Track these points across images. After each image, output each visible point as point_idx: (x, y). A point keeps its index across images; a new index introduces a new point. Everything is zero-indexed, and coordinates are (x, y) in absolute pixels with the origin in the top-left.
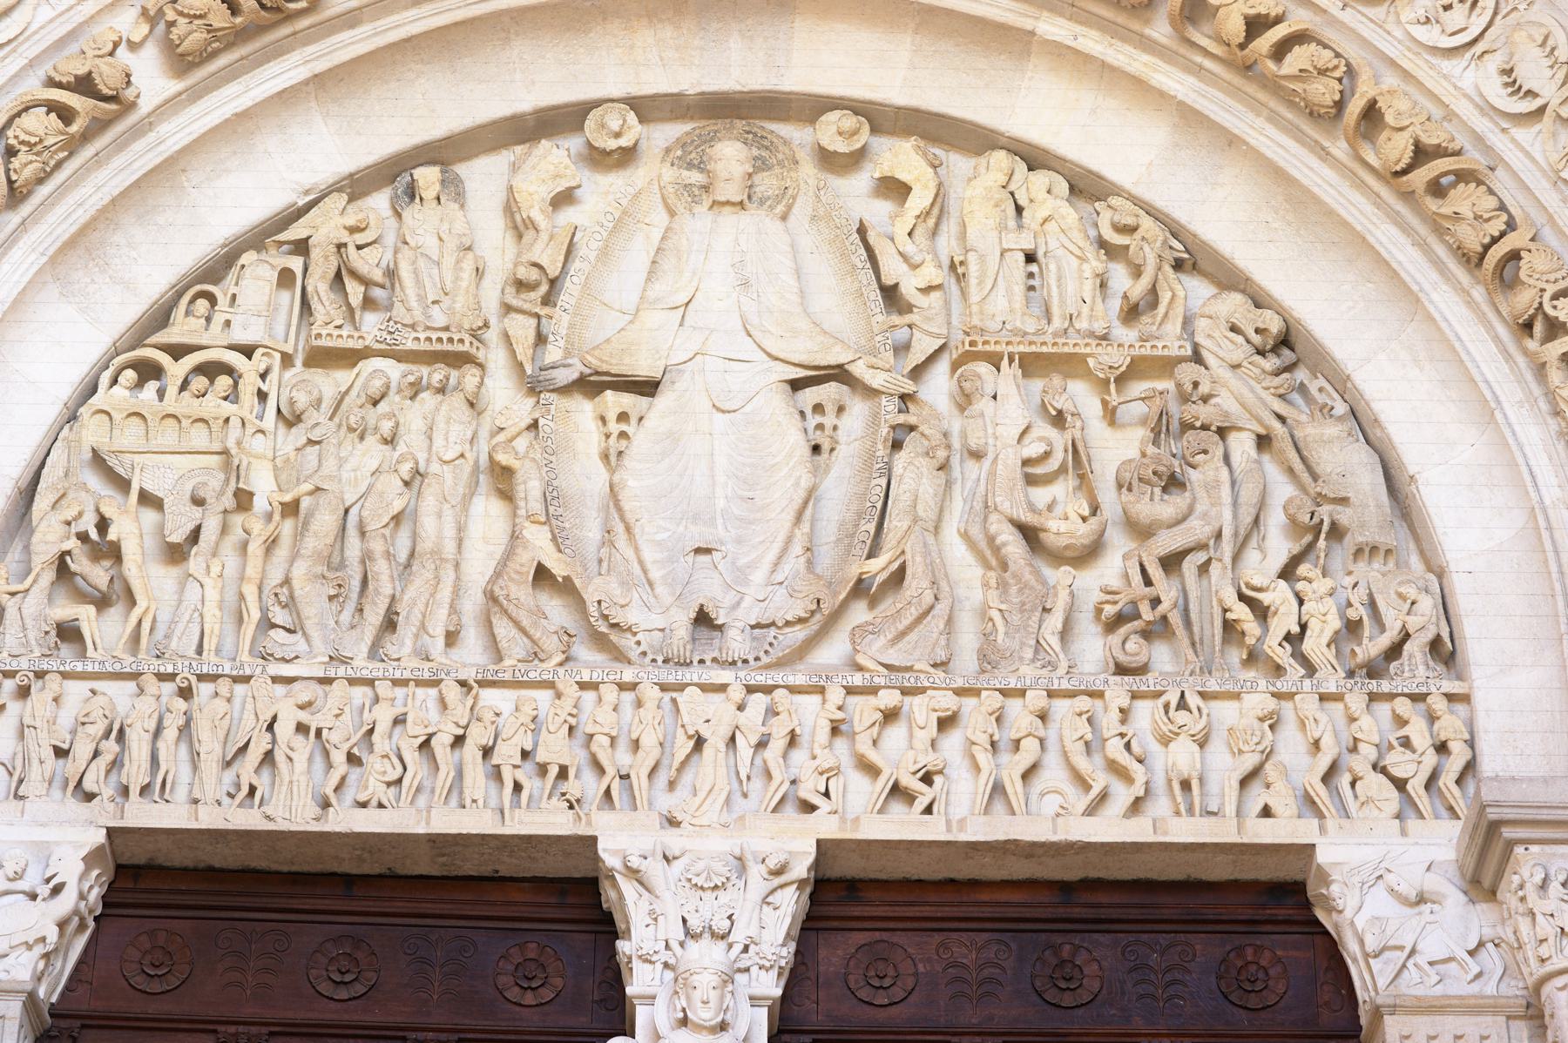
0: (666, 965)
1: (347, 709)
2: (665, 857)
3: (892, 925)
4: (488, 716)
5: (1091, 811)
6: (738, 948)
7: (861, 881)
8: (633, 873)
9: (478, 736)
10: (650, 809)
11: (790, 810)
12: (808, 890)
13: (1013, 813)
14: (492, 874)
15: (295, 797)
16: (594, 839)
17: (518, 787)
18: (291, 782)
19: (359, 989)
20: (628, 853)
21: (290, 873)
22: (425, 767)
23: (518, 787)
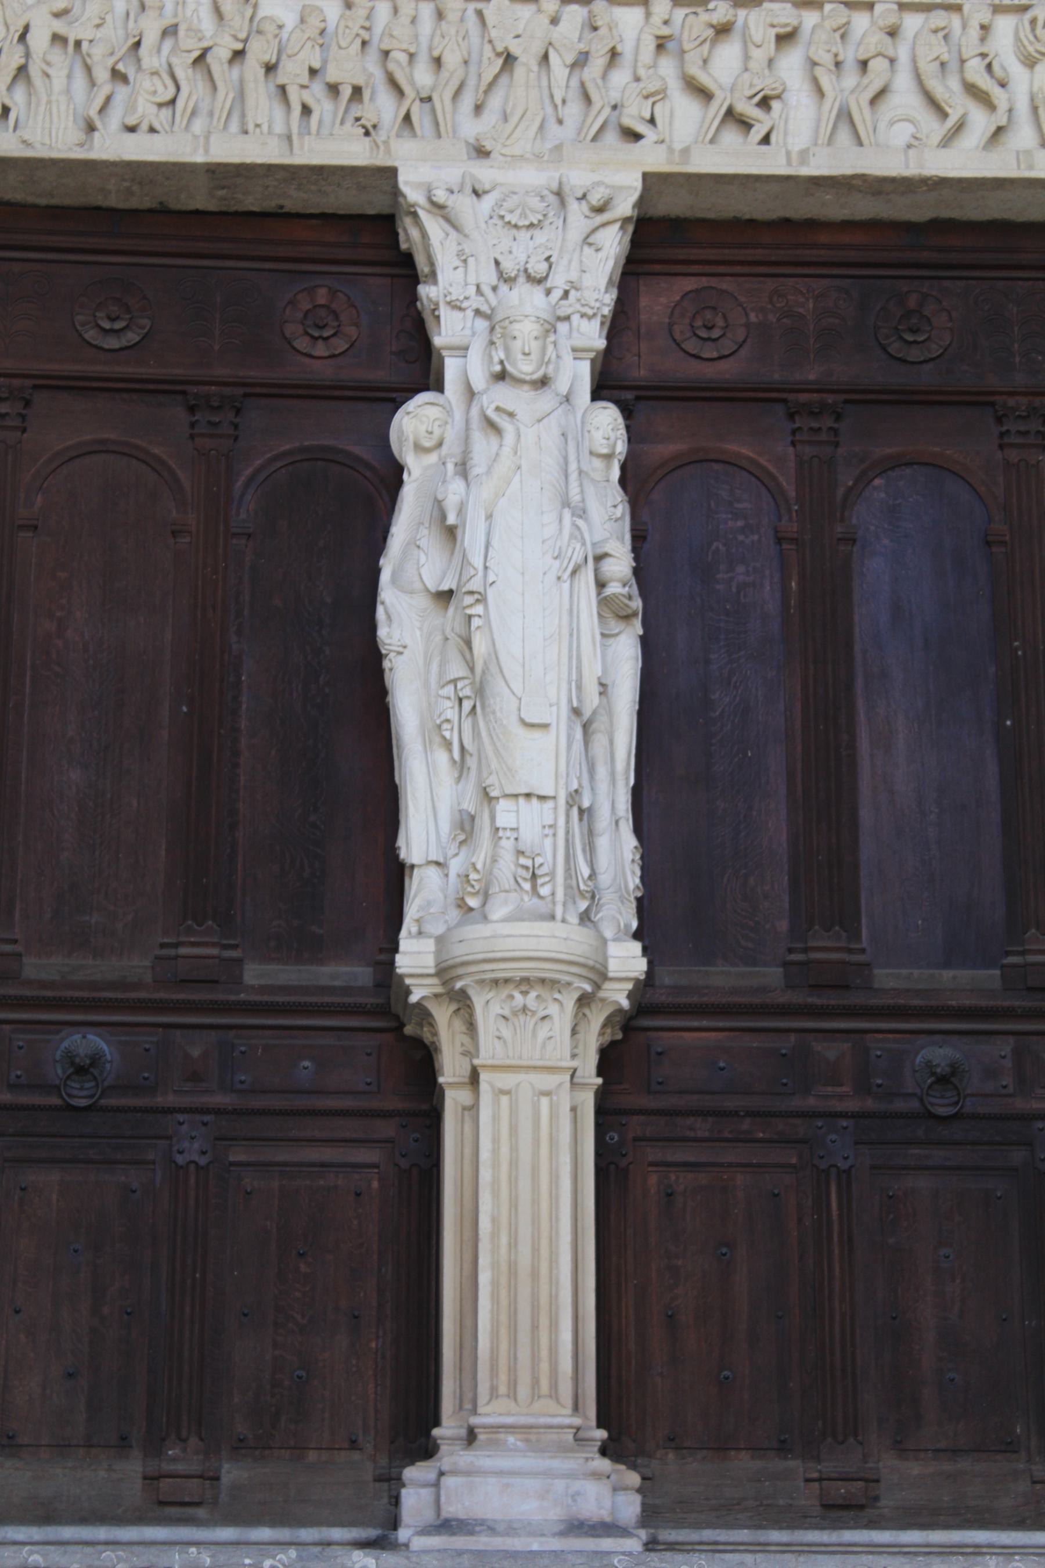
0: (478, 312)
1: (109, 18)
4: (270, 28)
5: (947, 142)
6: (557, 294)
8: (438, 208)
9: (259, 51)
10: (454, 137)
11: (611, 137)
12: (631, 229)
13: (860, 144)
15: (55, 119)
17: (306, 110)
18: (49, 102)
19: (132, 337)
21: (48, 207)
22: (200, 84)
23: (306, 110)
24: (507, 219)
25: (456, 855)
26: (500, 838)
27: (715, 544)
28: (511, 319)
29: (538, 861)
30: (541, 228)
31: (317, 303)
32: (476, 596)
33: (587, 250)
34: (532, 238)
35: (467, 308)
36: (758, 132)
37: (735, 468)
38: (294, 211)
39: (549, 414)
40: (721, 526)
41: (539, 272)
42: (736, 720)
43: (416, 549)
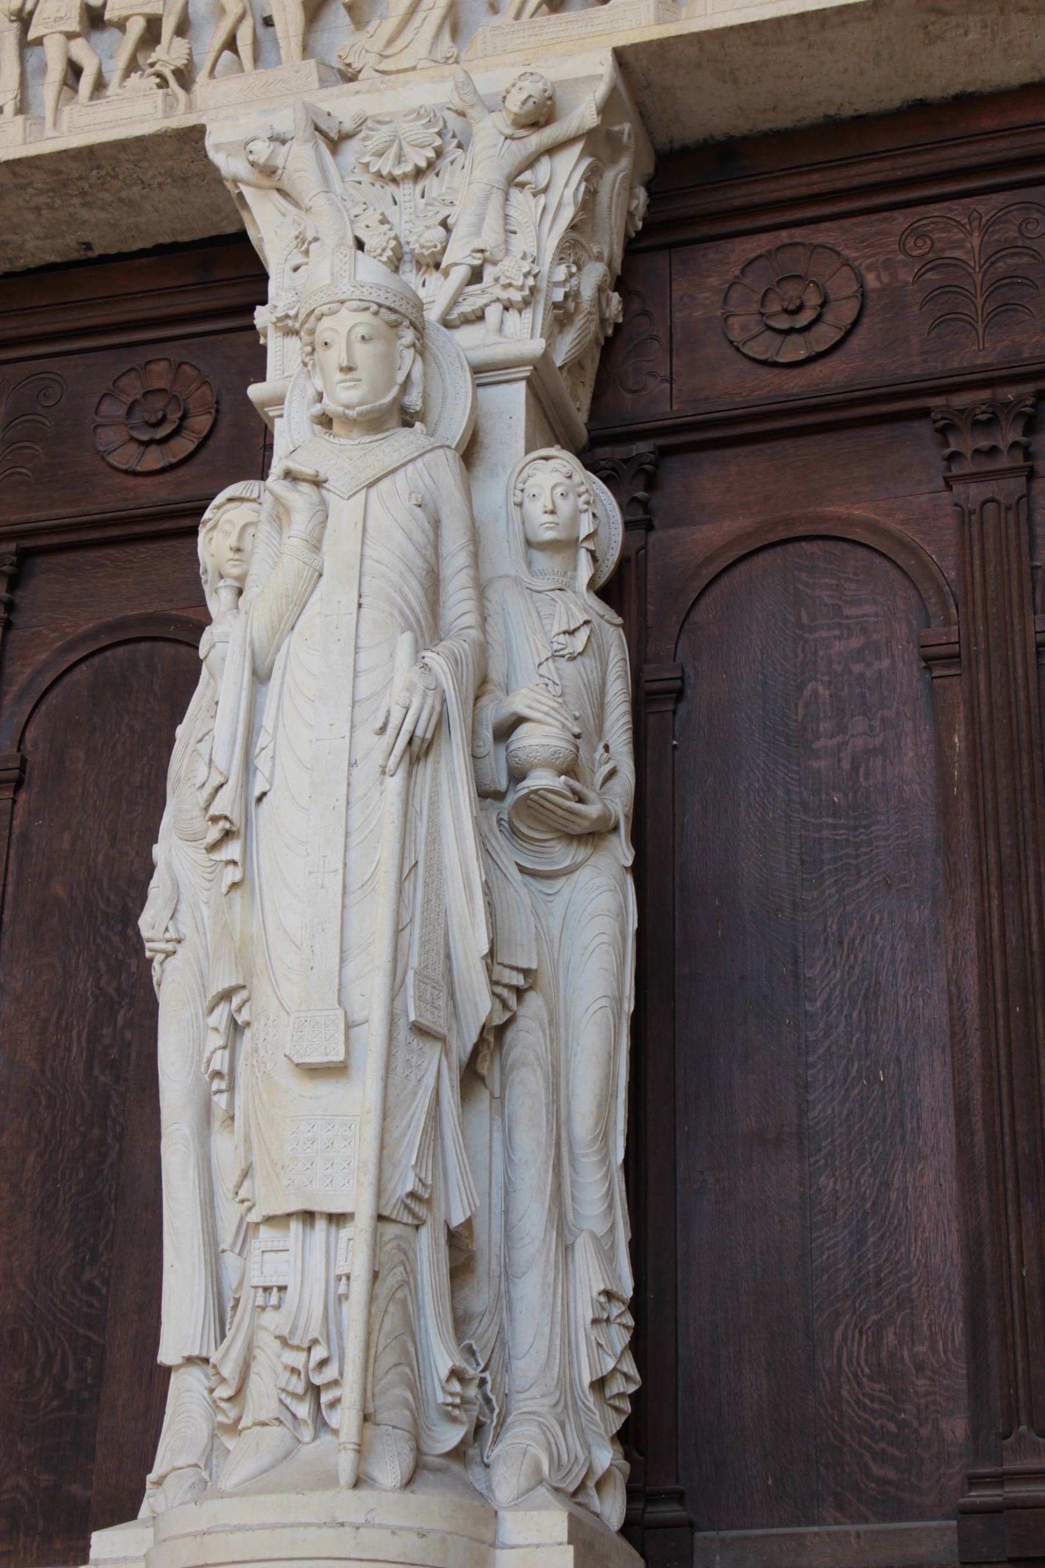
3: (810, 212)
6: (459, 274)
7: (745, 139)
14: (82, 255)
16: (199, 131)
23: (74, 70)
24: (373, 169)
28: (317, 312)
30: (437, 175)
32: (223, 824)
34: (423, 196)
37: (845, 545)
38: (112, 251)
39: (394, 471)
40: (821, 653)
41: (426, 244)
42: (855, 1015)
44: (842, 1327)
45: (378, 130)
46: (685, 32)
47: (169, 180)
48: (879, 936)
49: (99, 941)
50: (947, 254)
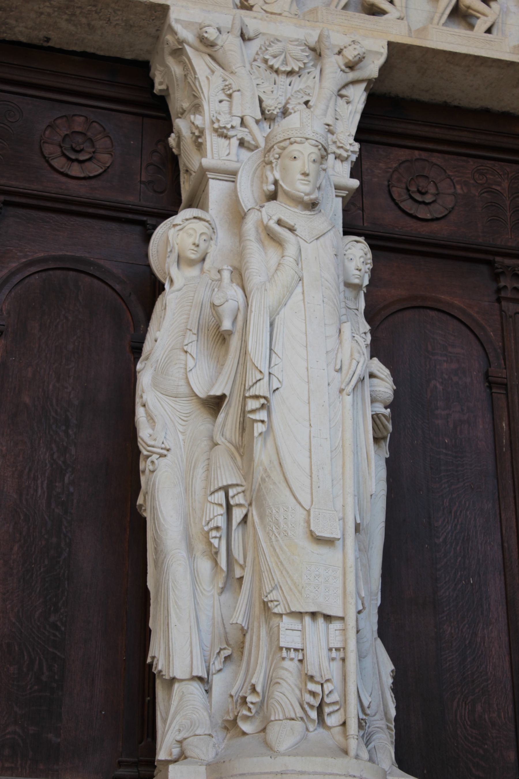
2: (242, 35)
3: (430, 146)
20: (203, 25)
24: (270, 63)
25: (220, 670)
26: (284, 659)
27: (433, 382)
28: (292, 140)
29: (328, 687)
30: (300, 76)
31: (74, 130)
33: (341, 102)
34: (290, 85)
35: (233, 136)
36: (481, 25)
37: (449, 317)
40: (438, 367)
42: (458, 548)
43: (183, 354)
44: (457, 700)
45: (276, 44)
46: (424, 45)
47: (123, 24)
48: (468, 512)
49: (51, 433)
50: (494, 187)
